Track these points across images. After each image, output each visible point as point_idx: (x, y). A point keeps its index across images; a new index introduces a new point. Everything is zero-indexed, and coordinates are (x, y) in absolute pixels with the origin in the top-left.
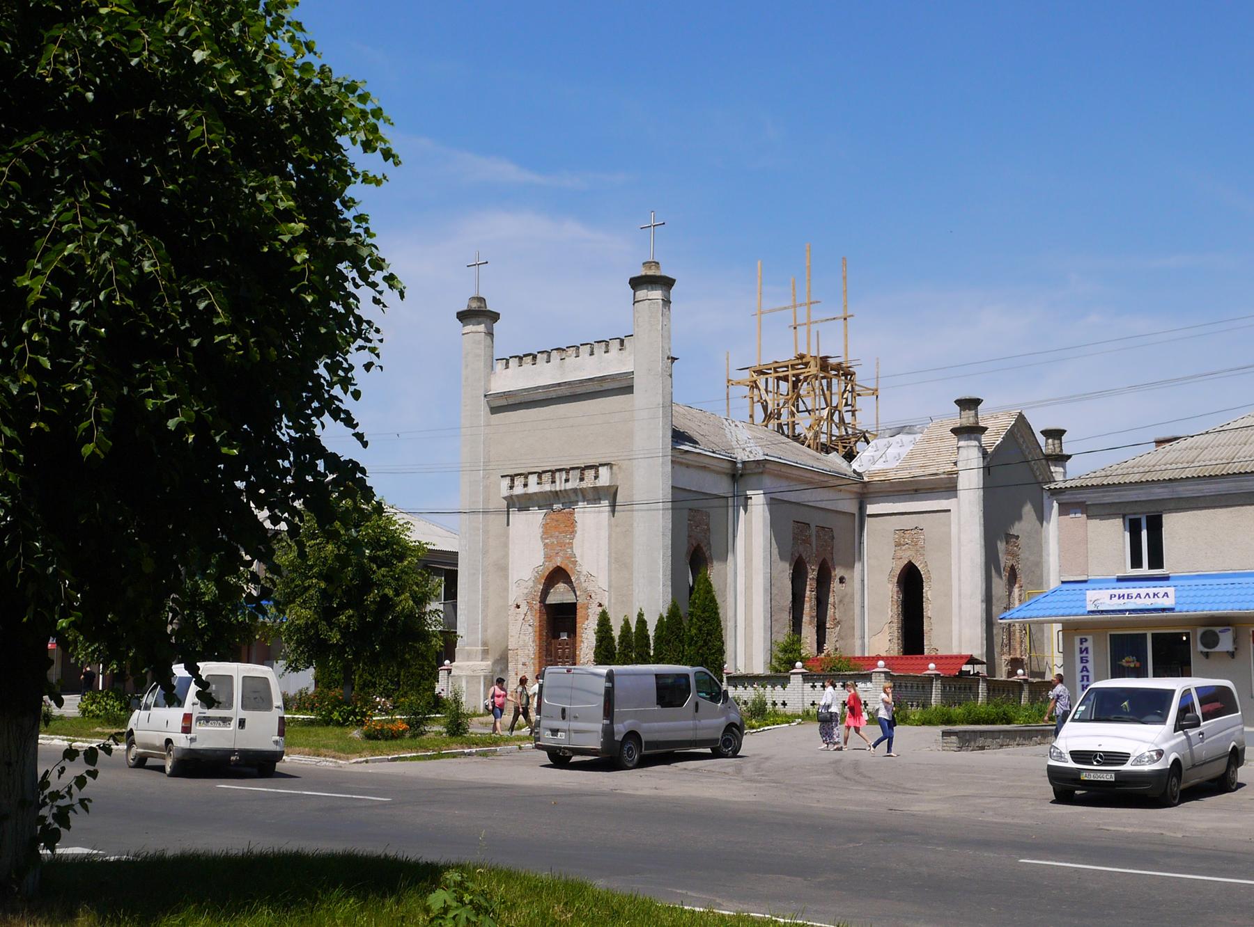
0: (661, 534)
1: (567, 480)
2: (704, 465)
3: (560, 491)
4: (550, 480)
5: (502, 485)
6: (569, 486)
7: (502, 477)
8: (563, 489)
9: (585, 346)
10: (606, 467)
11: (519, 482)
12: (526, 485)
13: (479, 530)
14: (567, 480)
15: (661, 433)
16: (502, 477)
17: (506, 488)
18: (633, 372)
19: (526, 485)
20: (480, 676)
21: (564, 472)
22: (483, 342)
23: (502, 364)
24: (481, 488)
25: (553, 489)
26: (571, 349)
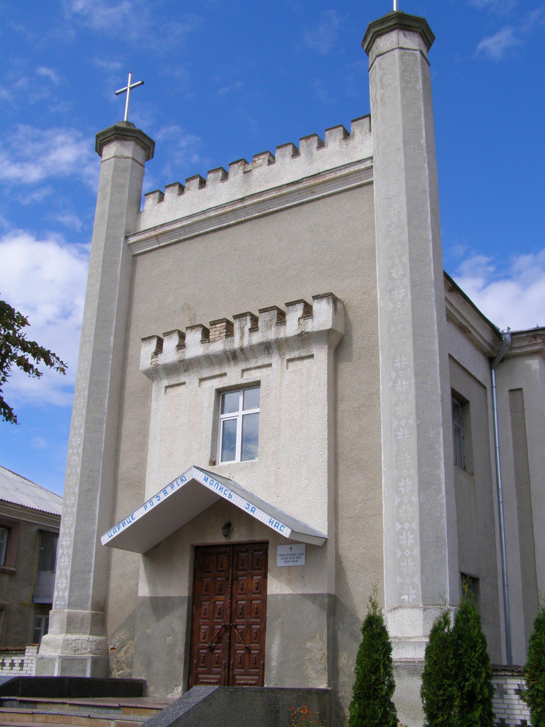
0: (440, 398)
1: (254, 329)
2: (465, 324)
3: (242, 349)
4: (224, 334)
5: (142, 353)
6: (257, 338)
7: (144, 339)
8: (246, 344)
9: (284, 149)
10: (324, 302)
11: (171, 344)
12: (181, 346)
13: (102, 424)
14: (254, 329)
15: (430, 233)
16: (144, 339)
17: (150, 357)
18: (371, 158)
19: (181, 346)
20: (83, 661)
21: (248, 318)
22: (129, 170)
23: (154, 199)
24: (110, 362)
25: (228, 348)
26: (262, 157)
